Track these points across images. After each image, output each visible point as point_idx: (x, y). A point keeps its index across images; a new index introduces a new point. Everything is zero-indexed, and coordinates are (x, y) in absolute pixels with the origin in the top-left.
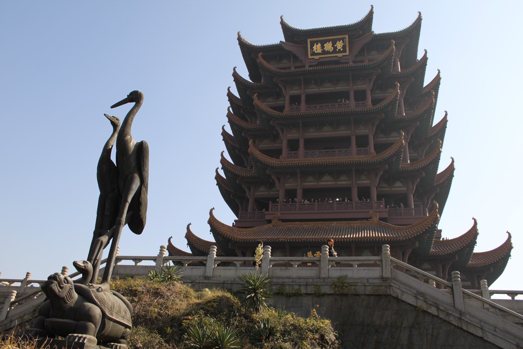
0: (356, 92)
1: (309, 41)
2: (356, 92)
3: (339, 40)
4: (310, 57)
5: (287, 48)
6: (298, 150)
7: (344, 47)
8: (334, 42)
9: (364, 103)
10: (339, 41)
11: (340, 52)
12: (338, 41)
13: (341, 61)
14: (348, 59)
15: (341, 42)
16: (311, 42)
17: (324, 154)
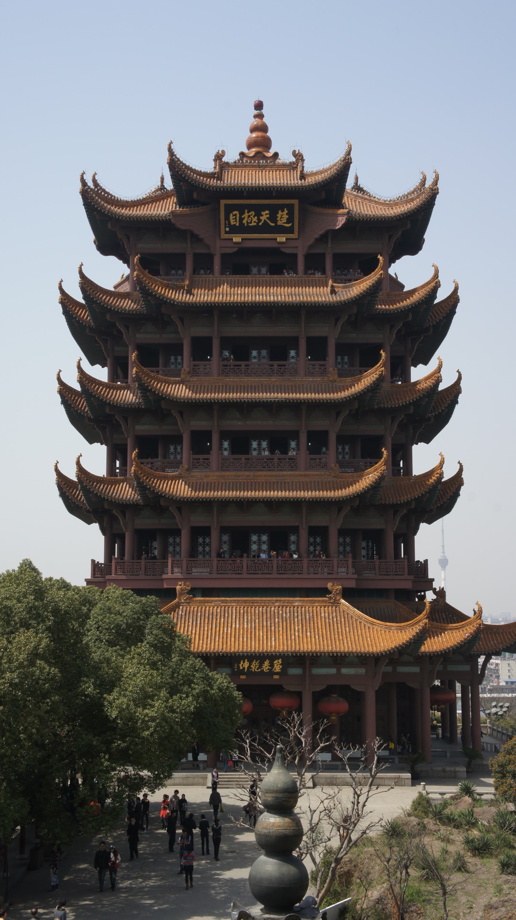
0: (310, 341)
1: (223, 202)
2: (310, 341)
3: (282, 207)
4: (224, 236)
5: (180, 225)
6: (209, 454)
7: (290, 220)
8: (274, 210)
9: (324, 365)
10: (283, 211)
11: (281, 230)
12: (280, 211)
13: (283, 250)
14: (297, 247)
15: (286, 211)
16: (226, 205)
17: (253, 462)
